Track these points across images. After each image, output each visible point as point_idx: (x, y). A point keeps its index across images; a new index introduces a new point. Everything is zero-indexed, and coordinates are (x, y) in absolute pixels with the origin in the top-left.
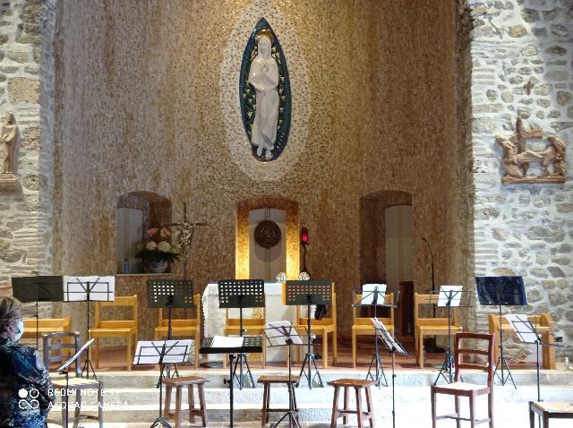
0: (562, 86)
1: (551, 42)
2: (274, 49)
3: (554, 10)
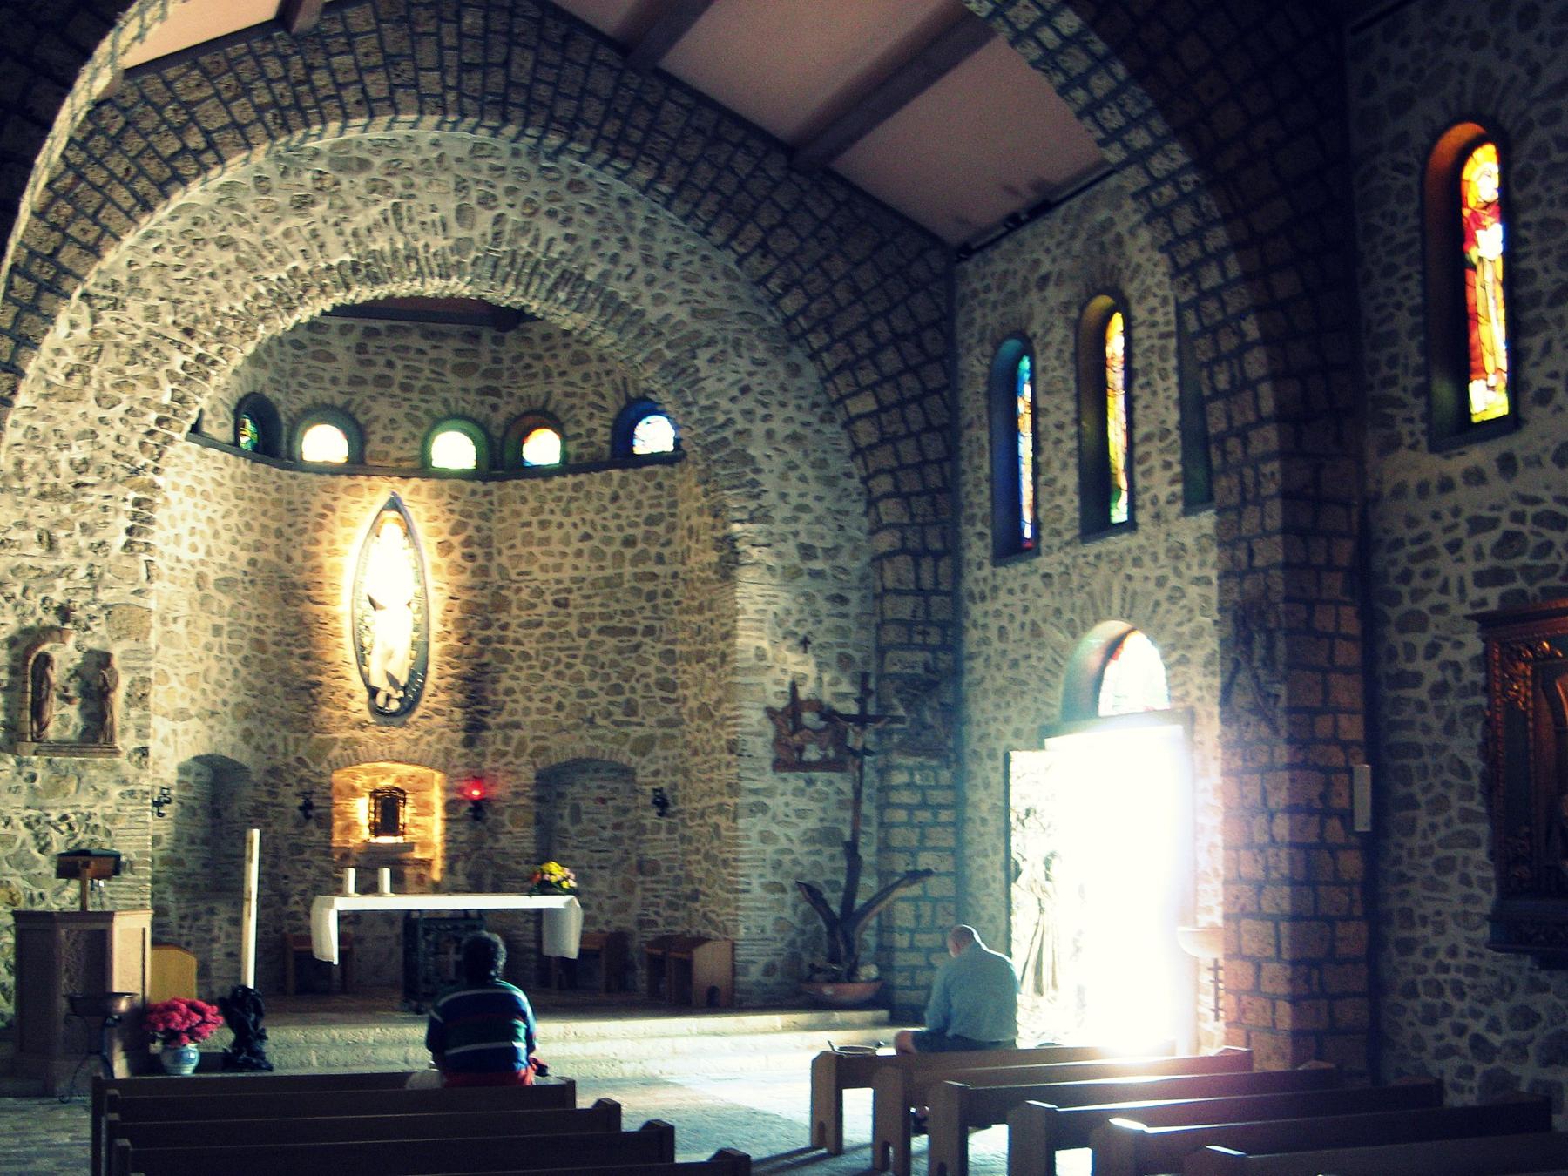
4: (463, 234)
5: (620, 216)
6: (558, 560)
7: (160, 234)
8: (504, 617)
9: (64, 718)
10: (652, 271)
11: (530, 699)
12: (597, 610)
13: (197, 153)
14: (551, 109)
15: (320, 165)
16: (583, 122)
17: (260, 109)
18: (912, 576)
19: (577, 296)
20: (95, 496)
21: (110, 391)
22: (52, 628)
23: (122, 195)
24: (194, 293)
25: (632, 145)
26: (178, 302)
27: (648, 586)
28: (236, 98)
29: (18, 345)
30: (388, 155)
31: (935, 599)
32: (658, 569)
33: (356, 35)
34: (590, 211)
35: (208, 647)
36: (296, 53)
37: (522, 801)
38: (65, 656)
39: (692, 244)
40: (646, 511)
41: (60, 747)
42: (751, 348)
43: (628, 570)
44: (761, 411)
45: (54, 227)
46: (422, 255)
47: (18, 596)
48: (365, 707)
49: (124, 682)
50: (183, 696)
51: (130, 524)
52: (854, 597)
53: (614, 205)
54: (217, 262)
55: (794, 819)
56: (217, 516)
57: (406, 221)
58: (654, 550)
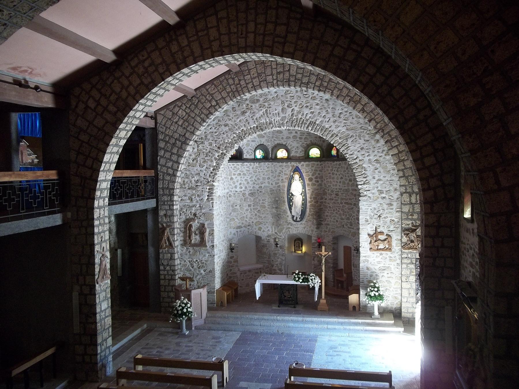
0: (391, 217)
1: (388, 201)
2: (300, 179)
3: (389, 190)
4: (284, 115)
5: (326, 105)
6: (336, 183)
7: (211, 125)
8: (326, 197)
9: (195, 239)
10: (335, 119)
11: (331, 218)
12: (344, 197)
13: (214, 106)
14: (301, 80)
15: (247, 102)
16: (310, 82)
17: (228, 93)
18: (408, 200)
19: (314, 128)
20: (200, 188)
21: (202, 164)
22: (192, 218)
23: (198, 119)
24: (220, 138)
25: (324, 87)
26: (216, 141)
28: (222, 91)
29: (178, 157)
30: (264, 97)
33: (251, 69)
34: (317, 104)
35: (247, 210)
36: (236, 77)
37: (330, 244)
38: (195, 225)
39: (346, 109)
41: (195, 245)
42: (364, 136)
45: (184, 128)
46: (273, 122)
47: (185, 212)
48: (291, 220)
49: (208, 230)
50: (239, 223)
51: (208, 194)
52: (395, 204)
53: (324, 101)
54: (224, 130)
55: (377, 264)
56: (248, 179)
57: (269, 114)
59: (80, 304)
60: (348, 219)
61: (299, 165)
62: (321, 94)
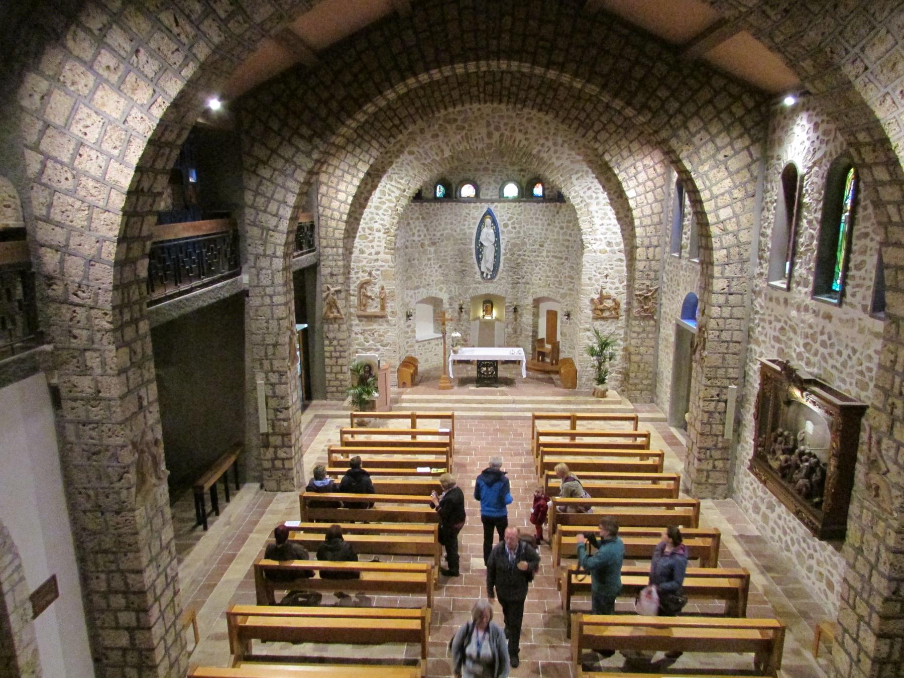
4: (489, 141)
13: (397, 127)
15: (441, 122)
17: (417, 109)
27: (566, 244)
31: (653, 262)
32: (570, 239)
34: (534, 128)
35: (426, 265)
40: (567, 218)
43: (561, 237)
44: (594, 195)
58: (569, 232)
59: (267, 397)
60: (556, 276)
61: (492, 207)
62: (541, 115)
